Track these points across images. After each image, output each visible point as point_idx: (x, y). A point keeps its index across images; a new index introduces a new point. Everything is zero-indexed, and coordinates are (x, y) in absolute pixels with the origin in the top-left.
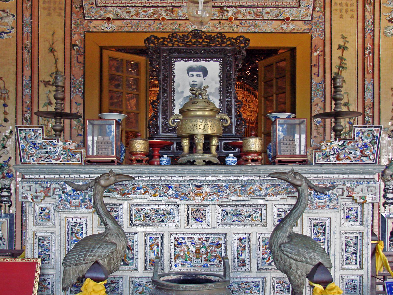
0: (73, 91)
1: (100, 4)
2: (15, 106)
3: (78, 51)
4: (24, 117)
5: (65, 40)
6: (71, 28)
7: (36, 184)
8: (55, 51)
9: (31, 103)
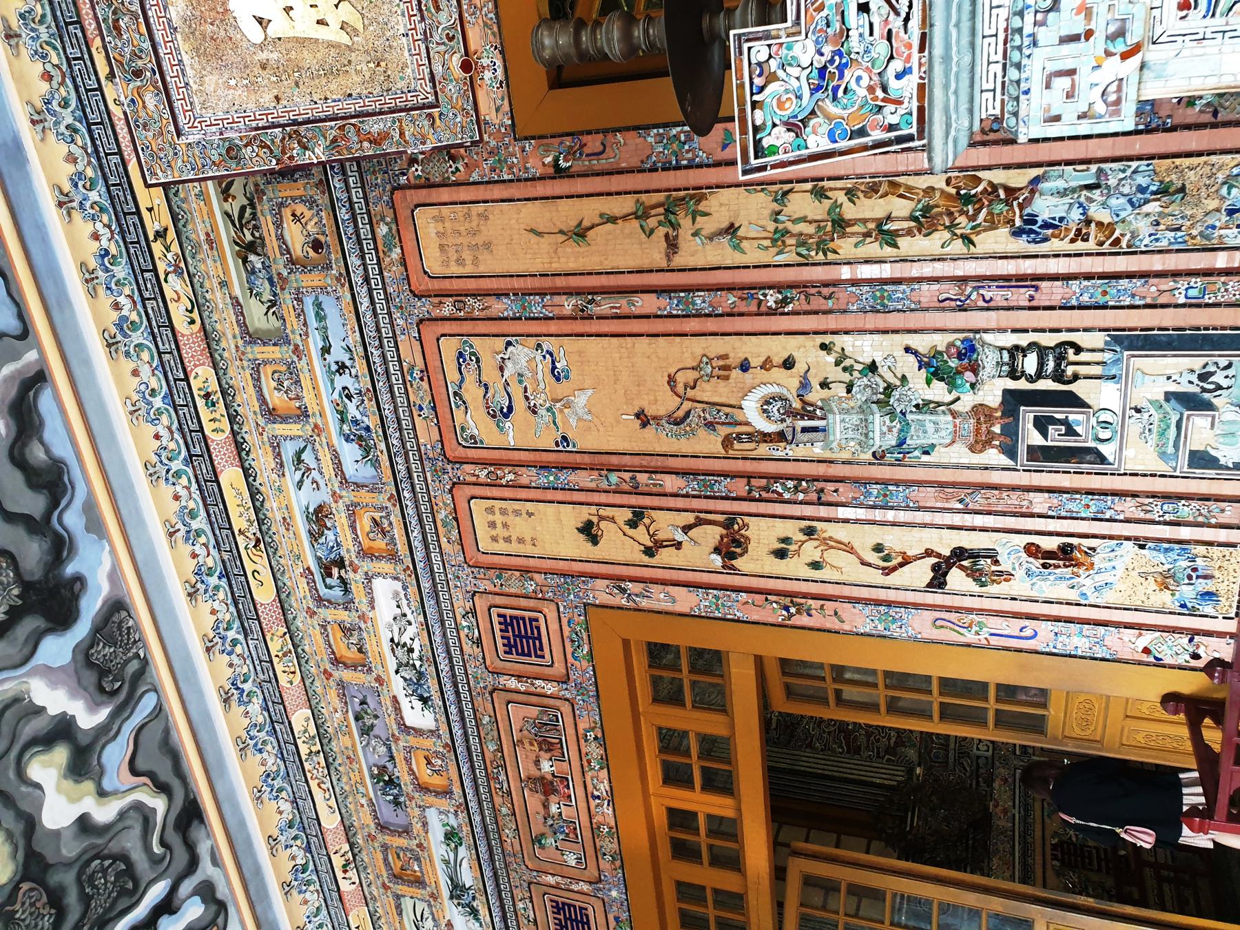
0: (689, 160)
1: (429, 96)
2: (744, 337)
3: (570, 153)
4: (776, 310)
5: (547, 198)
6: (511, 181)
7: (1035, 44)
8: (580, 224)
9: (734, 289)
